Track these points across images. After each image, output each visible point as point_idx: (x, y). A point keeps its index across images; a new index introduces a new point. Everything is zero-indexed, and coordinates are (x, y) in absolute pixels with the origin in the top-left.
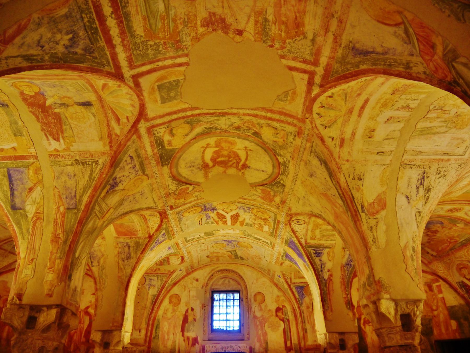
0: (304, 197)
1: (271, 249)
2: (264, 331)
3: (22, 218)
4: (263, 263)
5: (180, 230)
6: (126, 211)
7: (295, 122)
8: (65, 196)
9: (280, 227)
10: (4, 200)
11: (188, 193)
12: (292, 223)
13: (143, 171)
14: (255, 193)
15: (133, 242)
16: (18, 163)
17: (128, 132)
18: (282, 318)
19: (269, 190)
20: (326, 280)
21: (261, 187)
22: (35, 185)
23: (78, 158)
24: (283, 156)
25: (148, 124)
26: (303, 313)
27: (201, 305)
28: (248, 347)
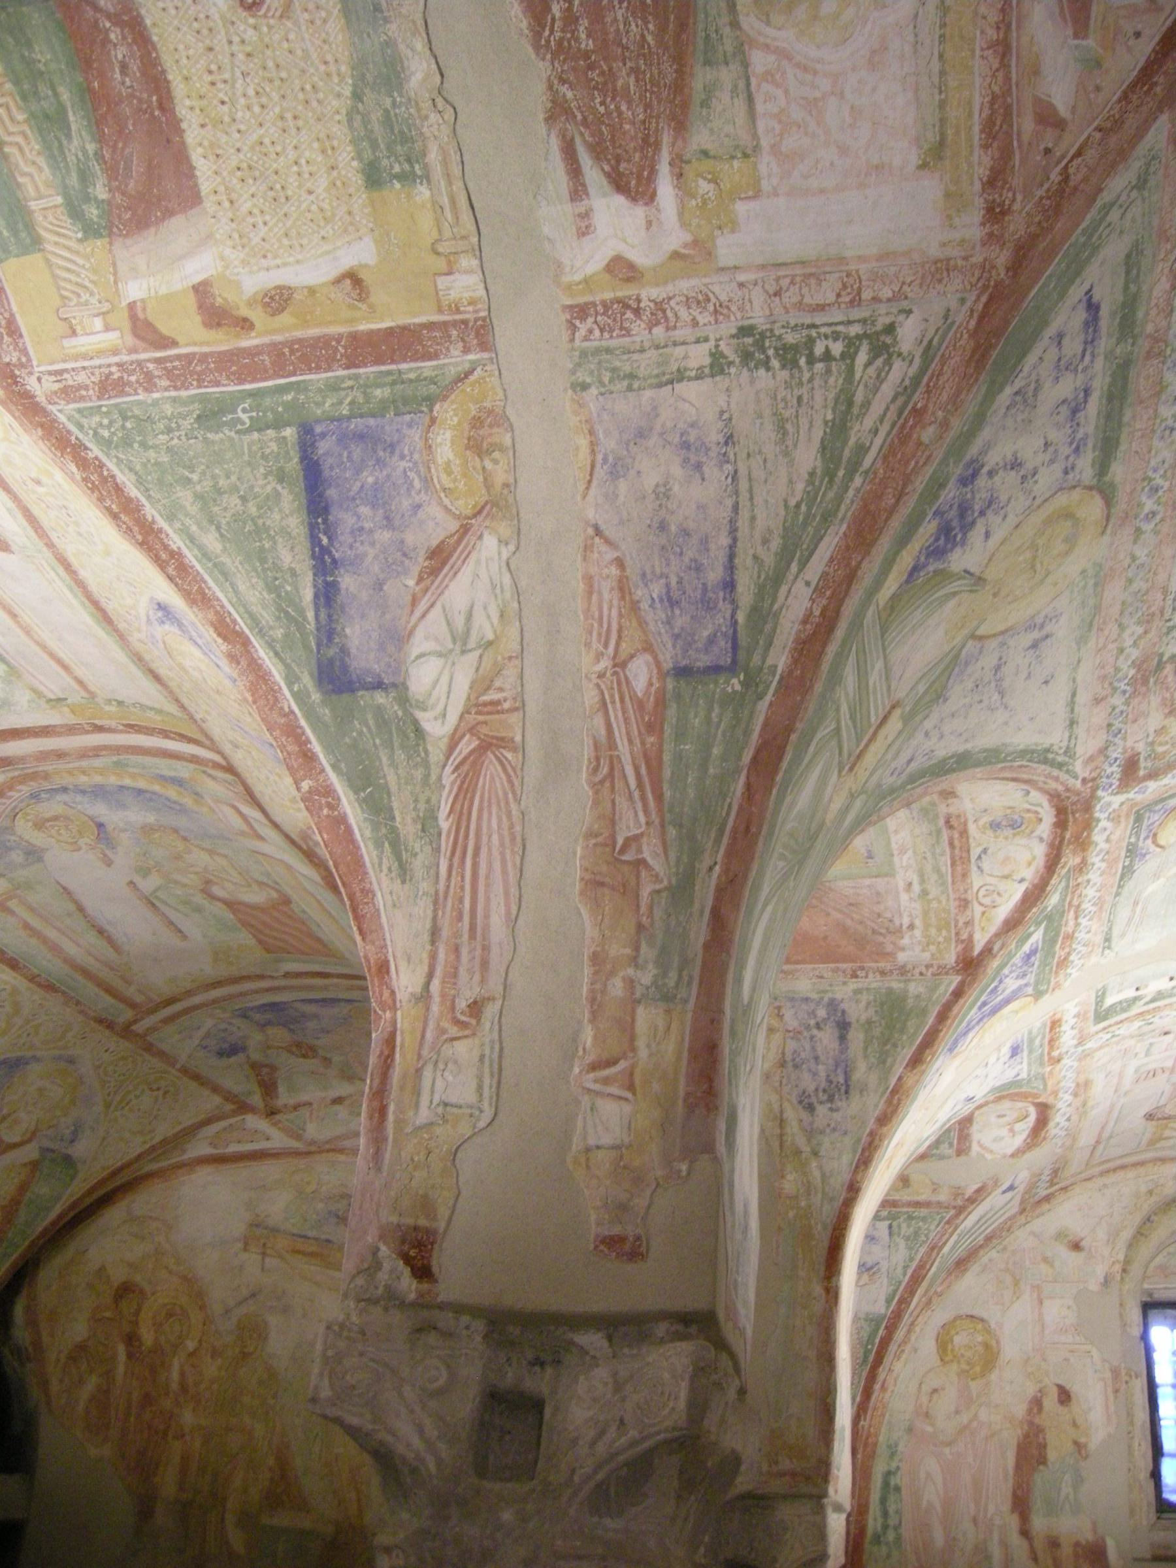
3: (389, 744)
5: (1099, 939)
8: (657, 589)
10: (279, 633)
15: (864, 998)
16: (366, 388)
17: (1133, 86)
22: (465, 530)
23: (758, 317)
27: (1108, 1375)
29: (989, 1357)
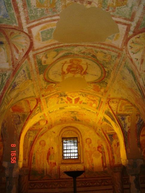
0: (118, 90)
1: (96, 116)
2: (91, 158)
4: (91, 122)
6: (20, 99)
7: (117, 50)
9: (102, 105)
11: (52, 88)
12: (110, 103)
13: (30, 77)
14: (89, 87)
15: (21, 115)
18: (100, 151)
19: (98, 85)
20: (127, 132)
21: (94, 84)
24: (108, 68)
25: (34, 53)
26: (113, 149)
28: (83, 166)
29: (45, 144)
